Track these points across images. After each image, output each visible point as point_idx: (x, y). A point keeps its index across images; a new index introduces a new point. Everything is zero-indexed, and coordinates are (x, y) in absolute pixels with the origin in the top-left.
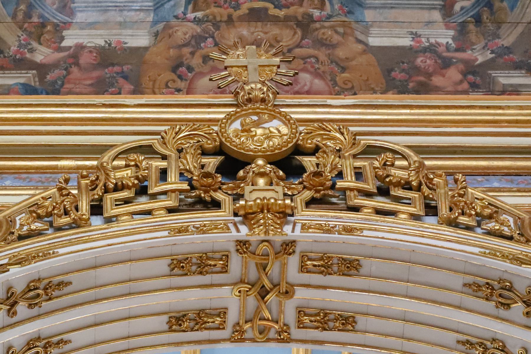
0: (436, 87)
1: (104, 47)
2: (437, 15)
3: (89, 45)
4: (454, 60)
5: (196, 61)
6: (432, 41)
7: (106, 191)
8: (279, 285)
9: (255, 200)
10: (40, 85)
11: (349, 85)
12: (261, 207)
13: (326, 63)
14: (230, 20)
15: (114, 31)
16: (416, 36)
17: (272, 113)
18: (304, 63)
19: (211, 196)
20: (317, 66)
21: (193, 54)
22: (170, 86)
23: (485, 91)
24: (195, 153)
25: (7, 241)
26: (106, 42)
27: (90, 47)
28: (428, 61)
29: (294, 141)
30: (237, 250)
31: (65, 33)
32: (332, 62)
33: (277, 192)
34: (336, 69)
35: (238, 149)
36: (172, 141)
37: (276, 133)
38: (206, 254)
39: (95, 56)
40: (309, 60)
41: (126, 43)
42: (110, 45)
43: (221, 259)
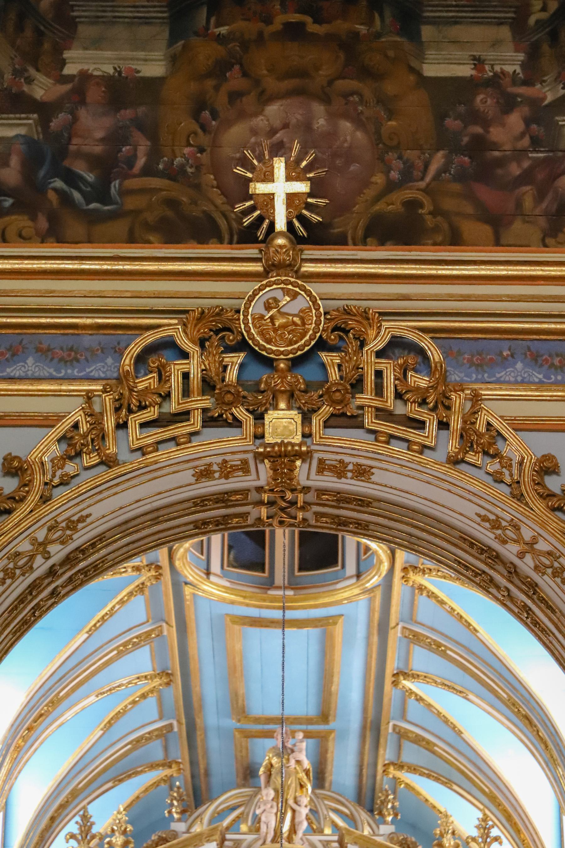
0: (495, 143)
1: (114, 76)
2: (505, 32)
3: (96, 73)
4: (519, 100)
5: (221, 100)
6: (497, 68)
7: (130, 411)
8: (296, 503)
9: (273, 445)
10: (43, 138)
11: (395, 143)
12: (278, 453)
13: (372, 104)
14: (260, 38)
15: (124, 53)
16: (478, 62)
17: (297, 289)
18: (346, 104)
19: (232, 414)
20: (360, 108)
21: (217, 88)
22: (191, 142)
23: (548, 151)
24: (216, 353)
25: (43, 499)
26: (115, 69)
27: (97, 77)
28: (489, 101)
29: (318, 335)
30: (257, 492)
31: (67, 54)
32: (378, 102)
33: (296, 422)
34: (382, 113)
35: (260, 350)
36: (193, 333)
37: (299, 326)
38: (227, 493)
39: (104, 92)
40: (351, 99)
41: (138, 72)
42: (120, 73)
43: (242, 495)
